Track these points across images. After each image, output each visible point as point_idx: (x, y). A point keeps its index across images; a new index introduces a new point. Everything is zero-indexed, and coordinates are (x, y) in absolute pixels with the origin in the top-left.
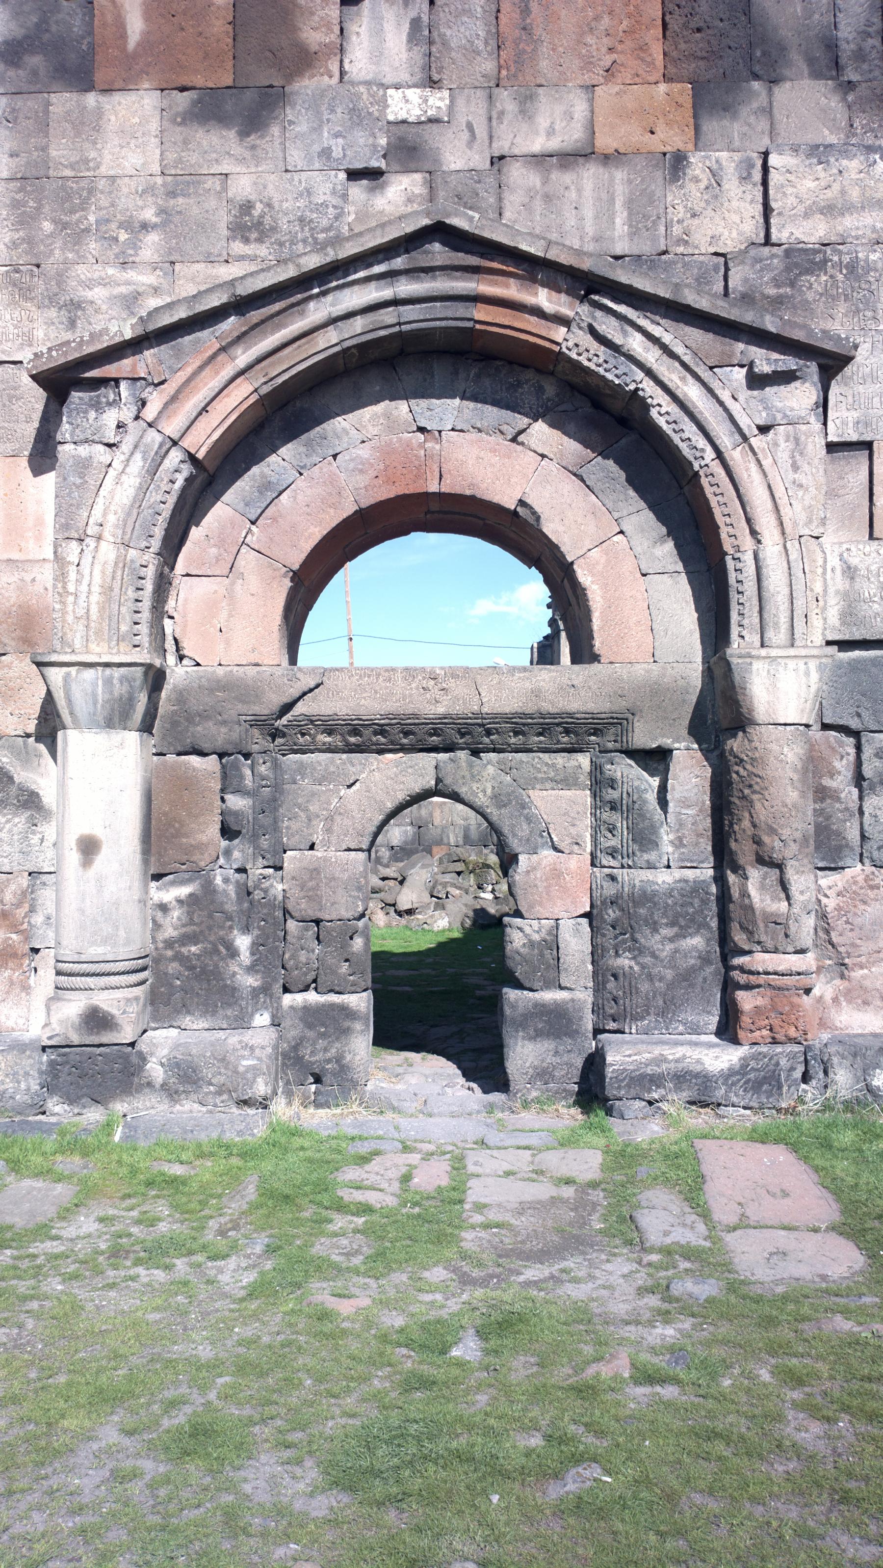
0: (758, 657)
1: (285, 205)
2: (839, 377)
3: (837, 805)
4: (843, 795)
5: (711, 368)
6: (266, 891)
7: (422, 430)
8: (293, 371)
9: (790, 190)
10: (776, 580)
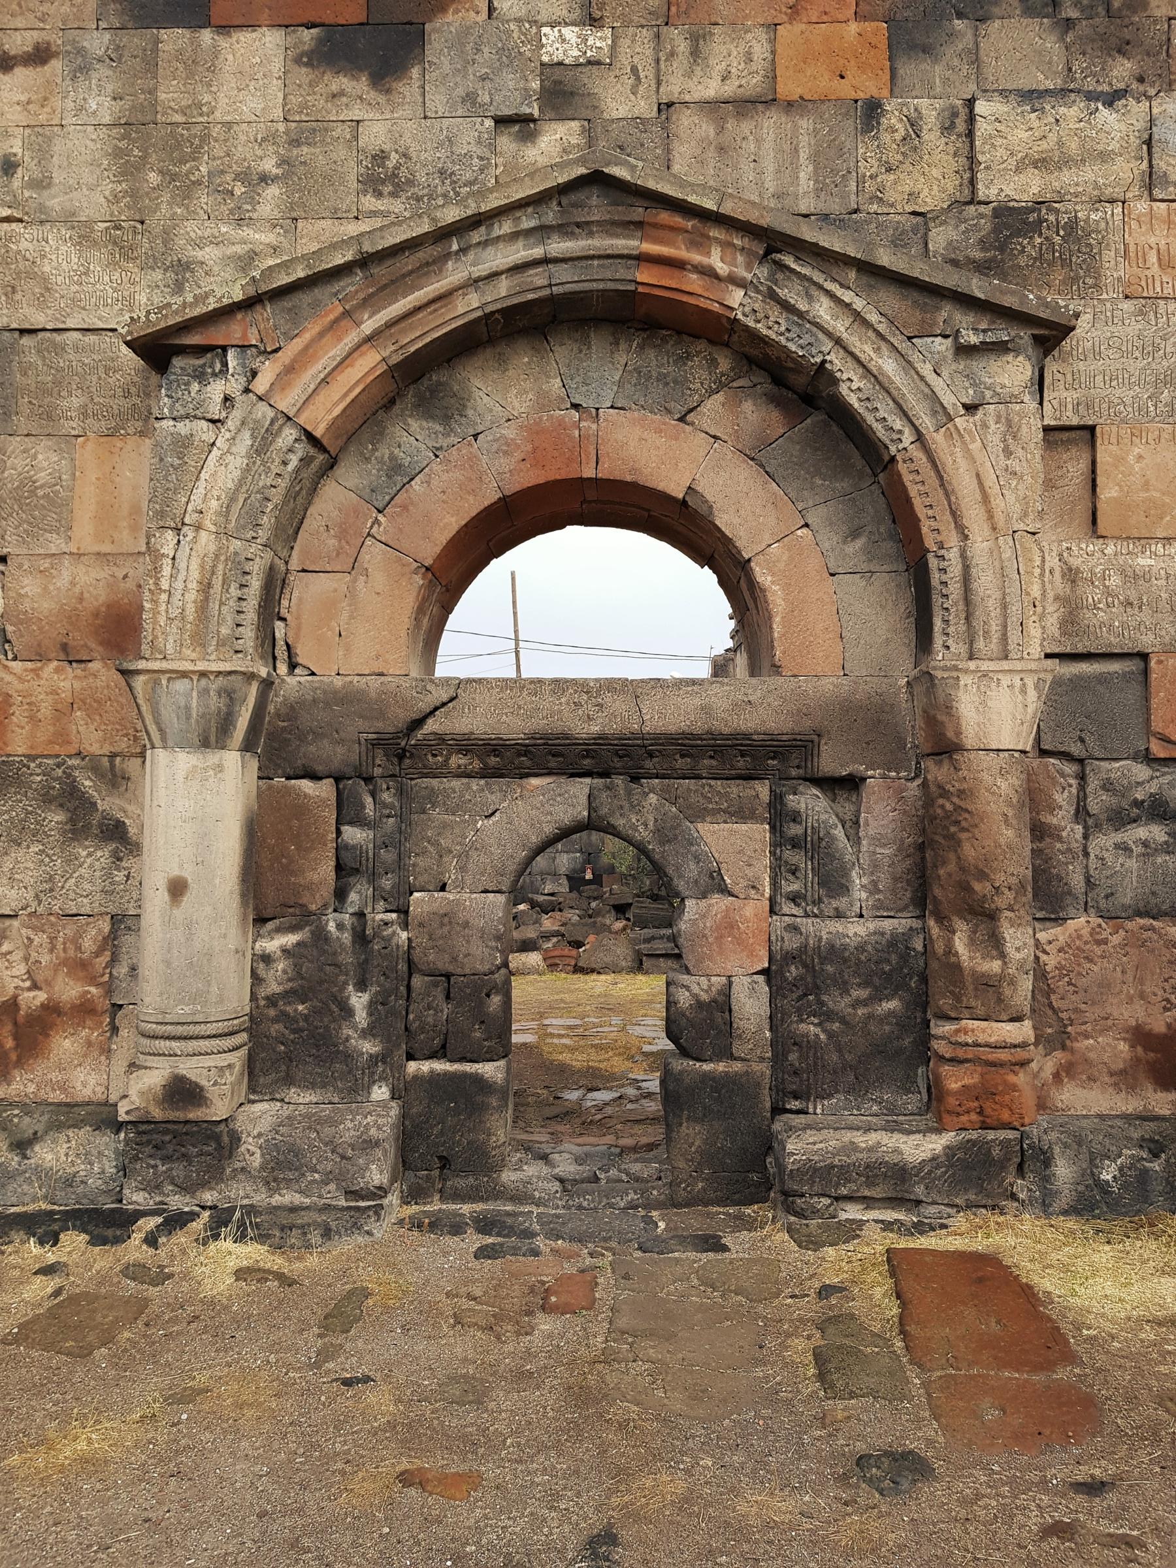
0: (966, 671)
1: (423, 156)
2: (1056, 353)
3: (1058, 845)
4: (1064, 834)
5: (909, 338)
6: (388, 939)
7: (576, 406)
8: (428, 339)
9: (999, 141)
10: (985, 583)
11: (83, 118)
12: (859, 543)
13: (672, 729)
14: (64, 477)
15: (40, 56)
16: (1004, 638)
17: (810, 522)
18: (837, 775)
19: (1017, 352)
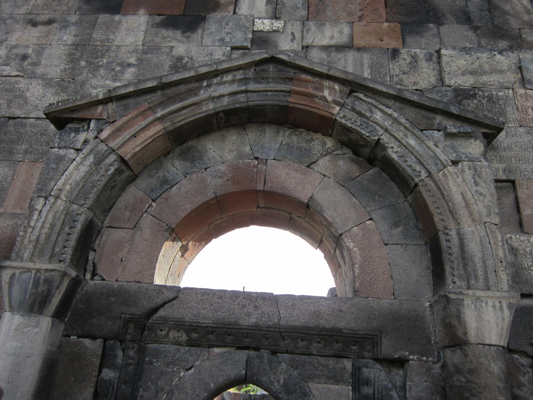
1: (199, 59)
5: (422, 130)
7: (256, 158)
8: (187, 121)
9: (453, 64)
10: (473, 247)
12: (399, 229)
13: (297, 324)
14: (8, 178)
15: (50, 22)
16: (486, 279)
17: (373, 217)
19: (476, 138)
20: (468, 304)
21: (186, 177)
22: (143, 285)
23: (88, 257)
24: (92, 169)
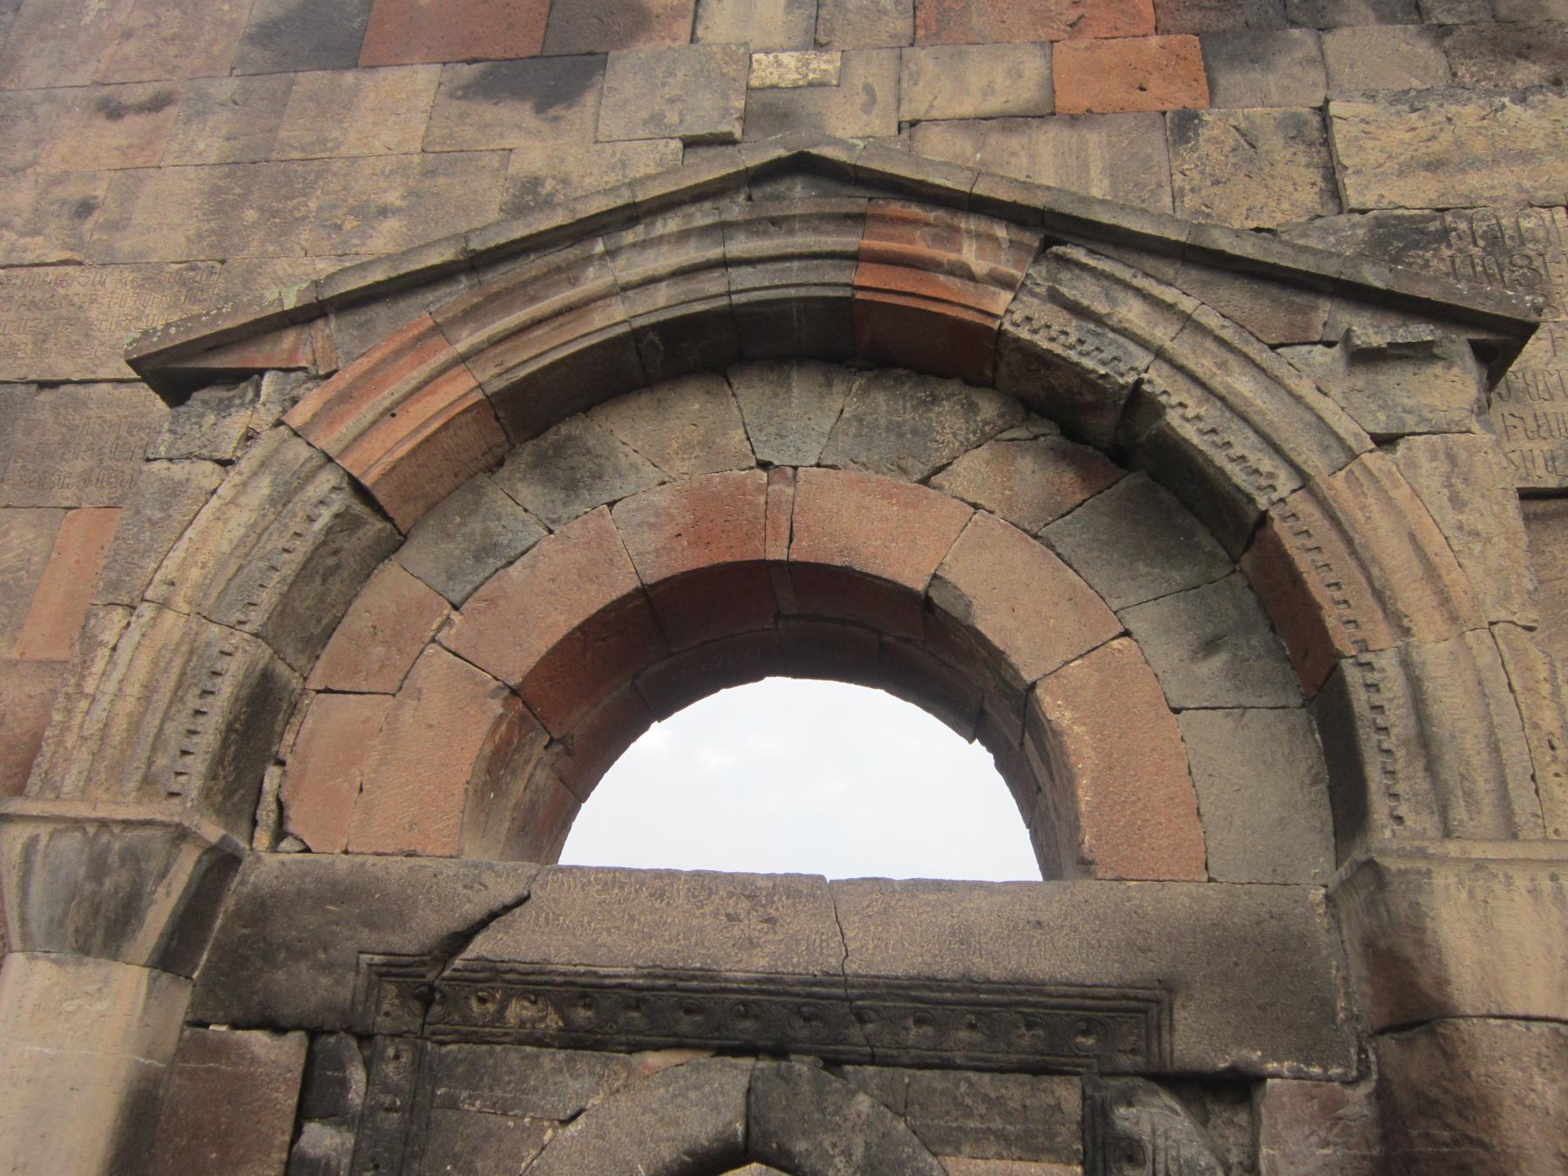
0: (1444, 860)
5: (1273, 347)
7: (764, 465)
8: (546, 361)
9: (1369, 144)
10: (1452, 705)
11: (187, 159)
12: (1218, 661)
13: (900, 969)
14: (35, 559)
15: (157, 104)
17: (1132, 627)
18: (1208, 1068)
20: (1447, 887)
21: (551, 532)
22: (423, 861)
23: (262, 782)
24: (264, 516)
